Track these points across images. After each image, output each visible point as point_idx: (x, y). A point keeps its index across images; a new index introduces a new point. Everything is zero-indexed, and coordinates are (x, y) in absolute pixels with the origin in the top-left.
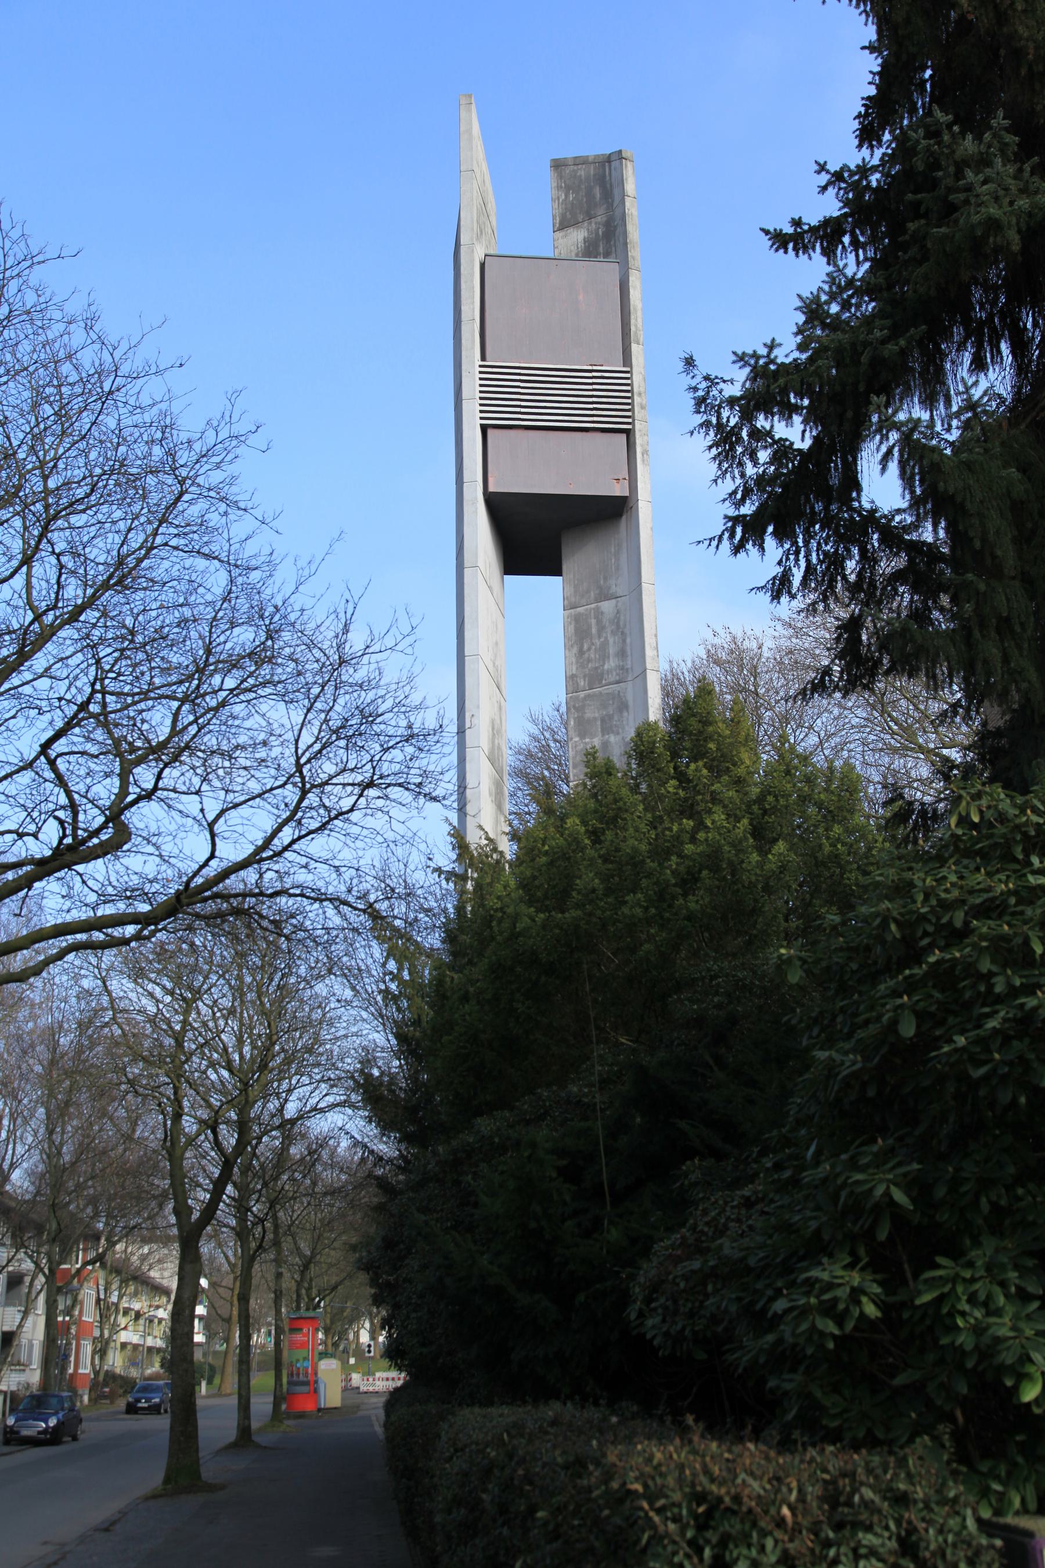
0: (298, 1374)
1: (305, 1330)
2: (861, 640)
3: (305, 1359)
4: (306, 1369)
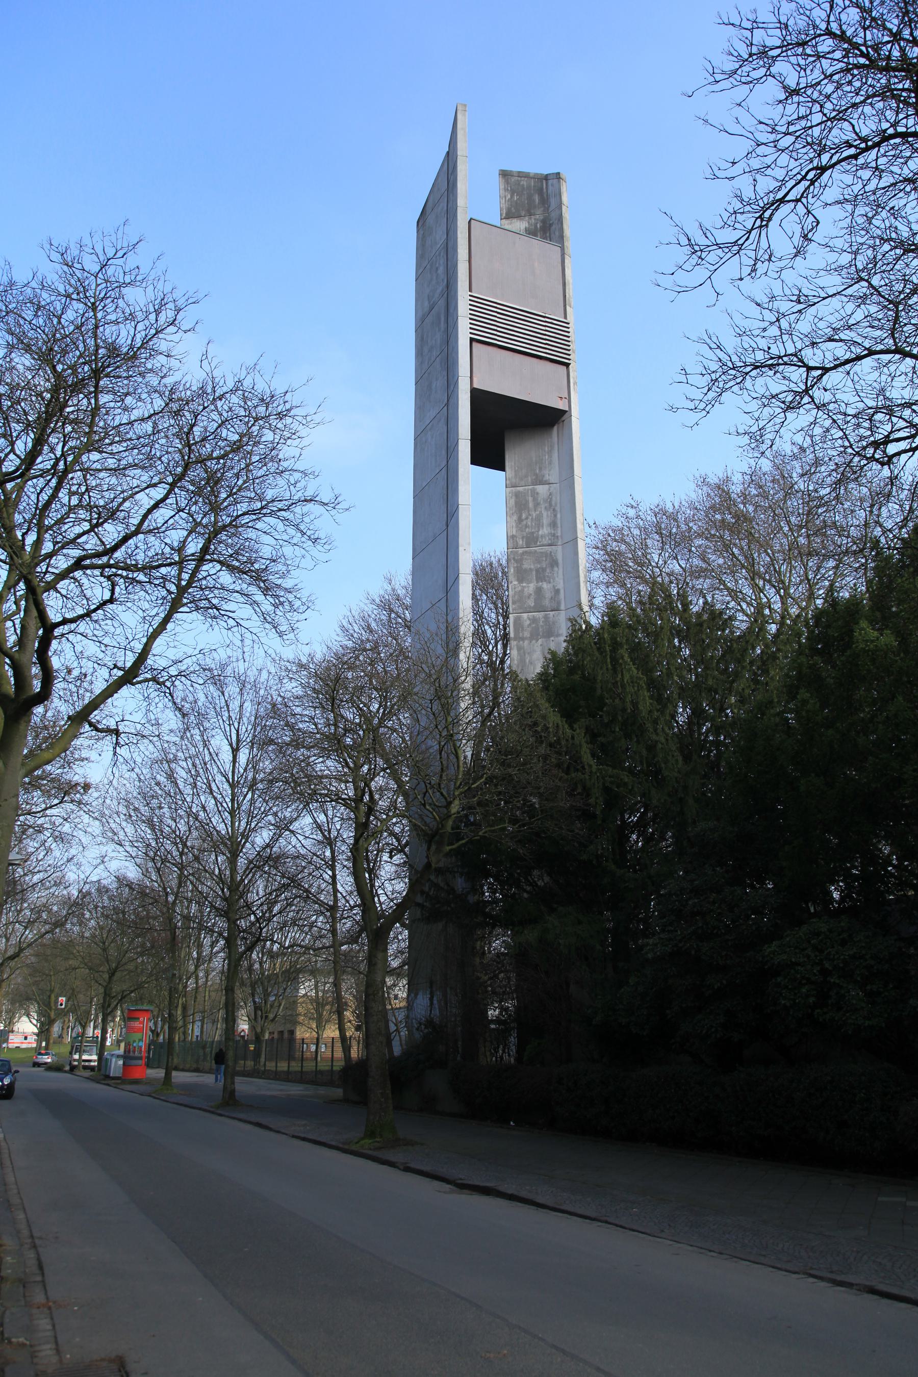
0: (134, 1052)
1: (141, 1019)
2: (39, 643)
3: (140, 1040)
4: (141, 1047)
